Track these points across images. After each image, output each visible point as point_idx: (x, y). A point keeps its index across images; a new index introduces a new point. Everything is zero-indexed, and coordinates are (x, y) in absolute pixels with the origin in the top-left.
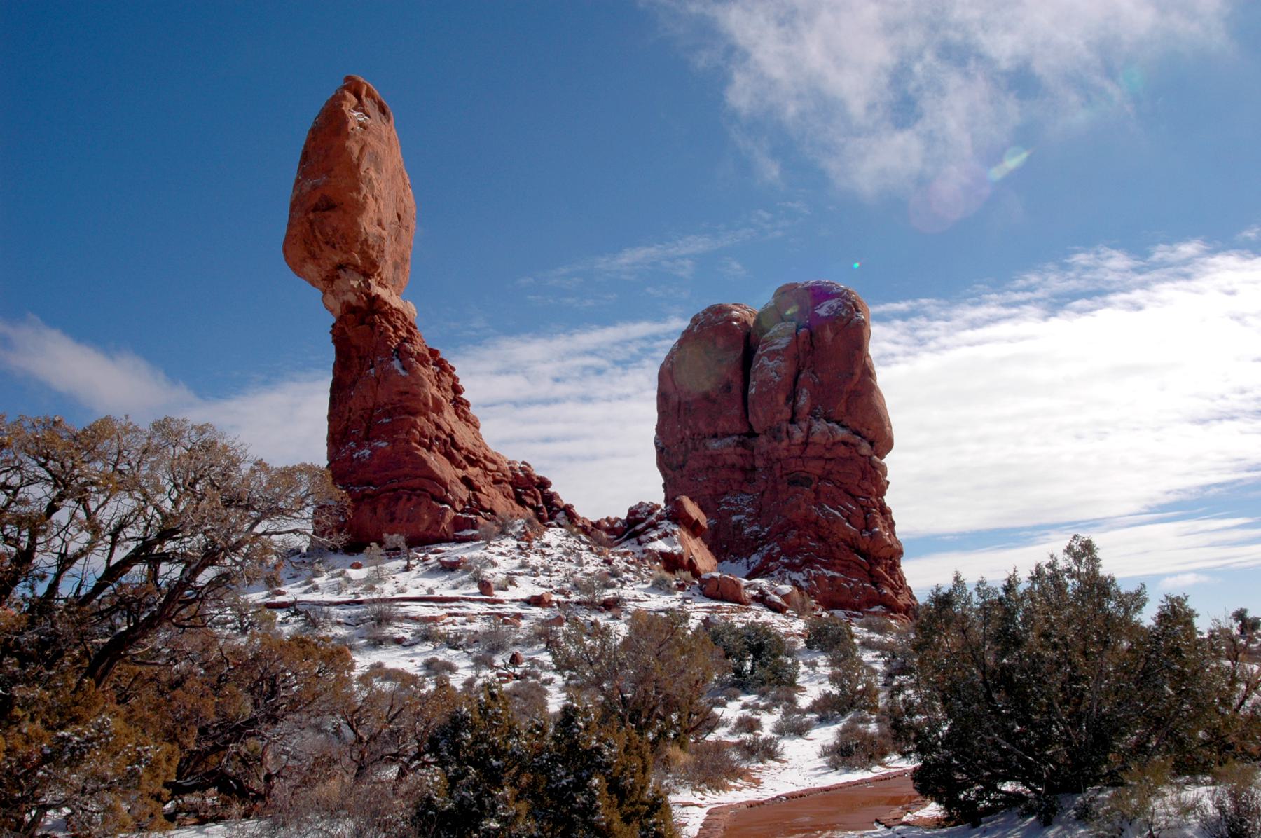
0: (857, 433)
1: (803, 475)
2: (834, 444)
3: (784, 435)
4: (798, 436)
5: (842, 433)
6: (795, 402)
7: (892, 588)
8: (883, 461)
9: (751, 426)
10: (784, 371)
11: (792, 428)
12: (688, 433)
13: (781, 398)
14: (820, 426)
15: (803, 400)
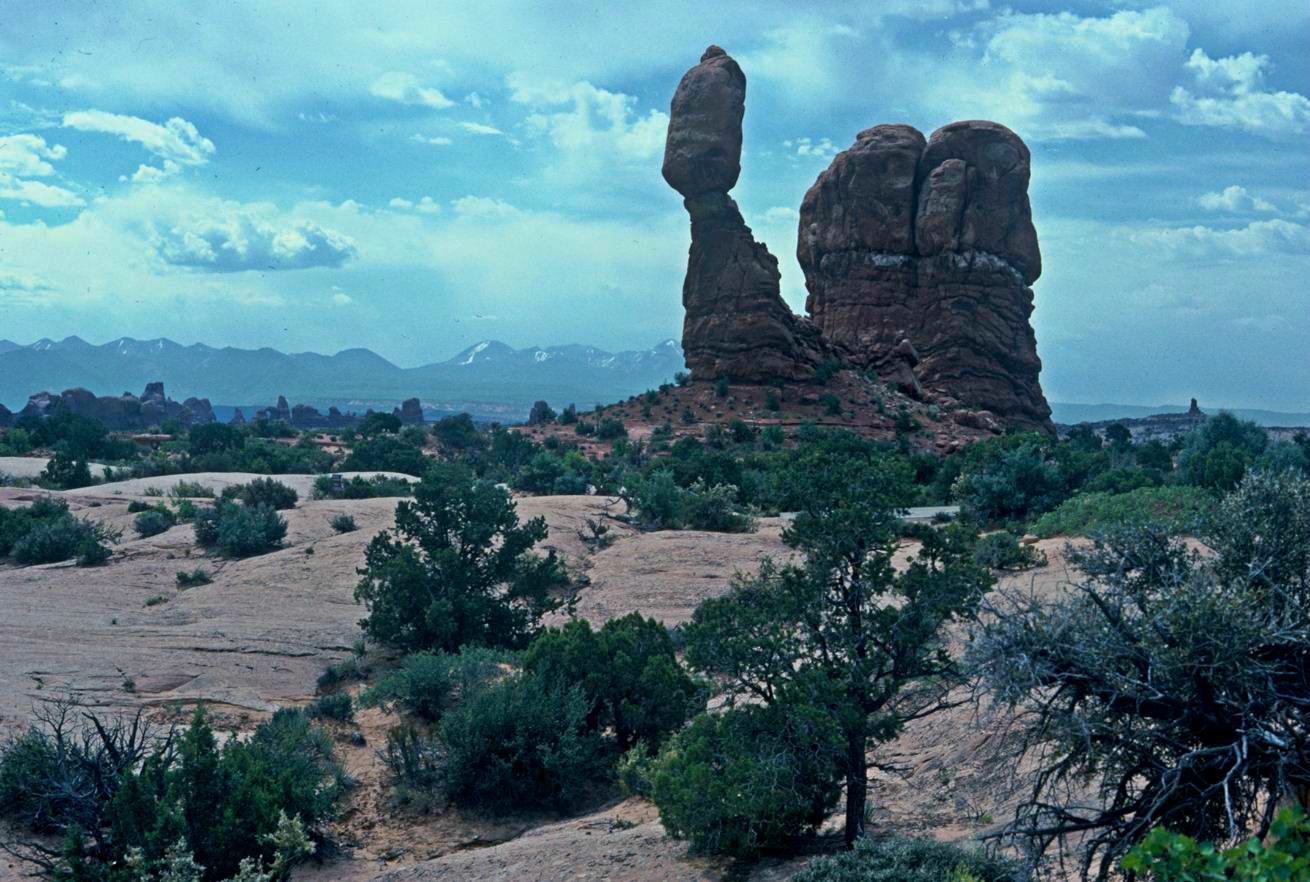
0: (1012, 264)
1: (965, 299)
2: (994, 272)
3: (951, 265)
4: (963, 264)
5: (1002, 264)
6: (962, 234)
7: (1031, 398)
8: (1031, 287)
9: (916, 248)
10: (954, 207)
11: (958, 258)
12: (853, 244)
13: (950, 231)
14: (981, 259)
15: (969, 236)
